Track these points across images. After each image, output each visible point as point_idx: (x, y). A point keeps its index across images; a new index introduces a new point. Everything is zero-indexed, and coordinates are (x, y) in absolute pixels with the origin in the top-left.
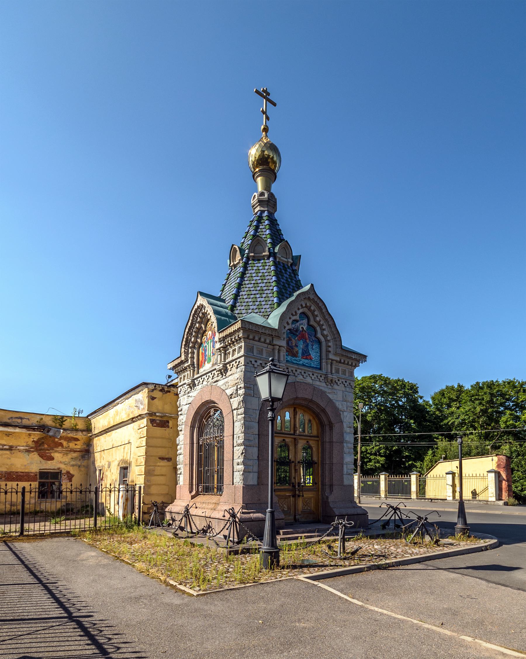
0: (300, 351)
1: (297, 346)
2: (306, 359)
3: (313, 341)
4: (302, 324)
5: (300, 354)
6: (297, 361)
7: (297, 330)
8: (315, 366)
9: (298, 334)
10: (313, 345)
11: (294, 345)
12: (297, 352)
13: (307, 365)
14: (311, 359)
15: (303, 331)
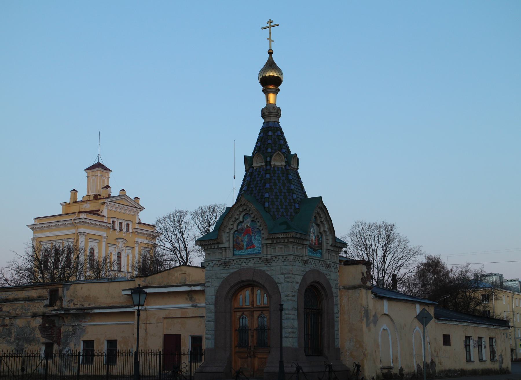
0: (245, 244)
1: (242, 241)
2: (250, 248)
3: (256, 232)
4: (247, 222)
5: (245, 247)
6: (243, 252)
7: (243, 229)
8: (258, 252)
9: (243, 232)
10: (255, 236)
11: (240, 241)
12: (243, 246)
13: (251, 253)
14: (254, 247)
15: (247, 228)
